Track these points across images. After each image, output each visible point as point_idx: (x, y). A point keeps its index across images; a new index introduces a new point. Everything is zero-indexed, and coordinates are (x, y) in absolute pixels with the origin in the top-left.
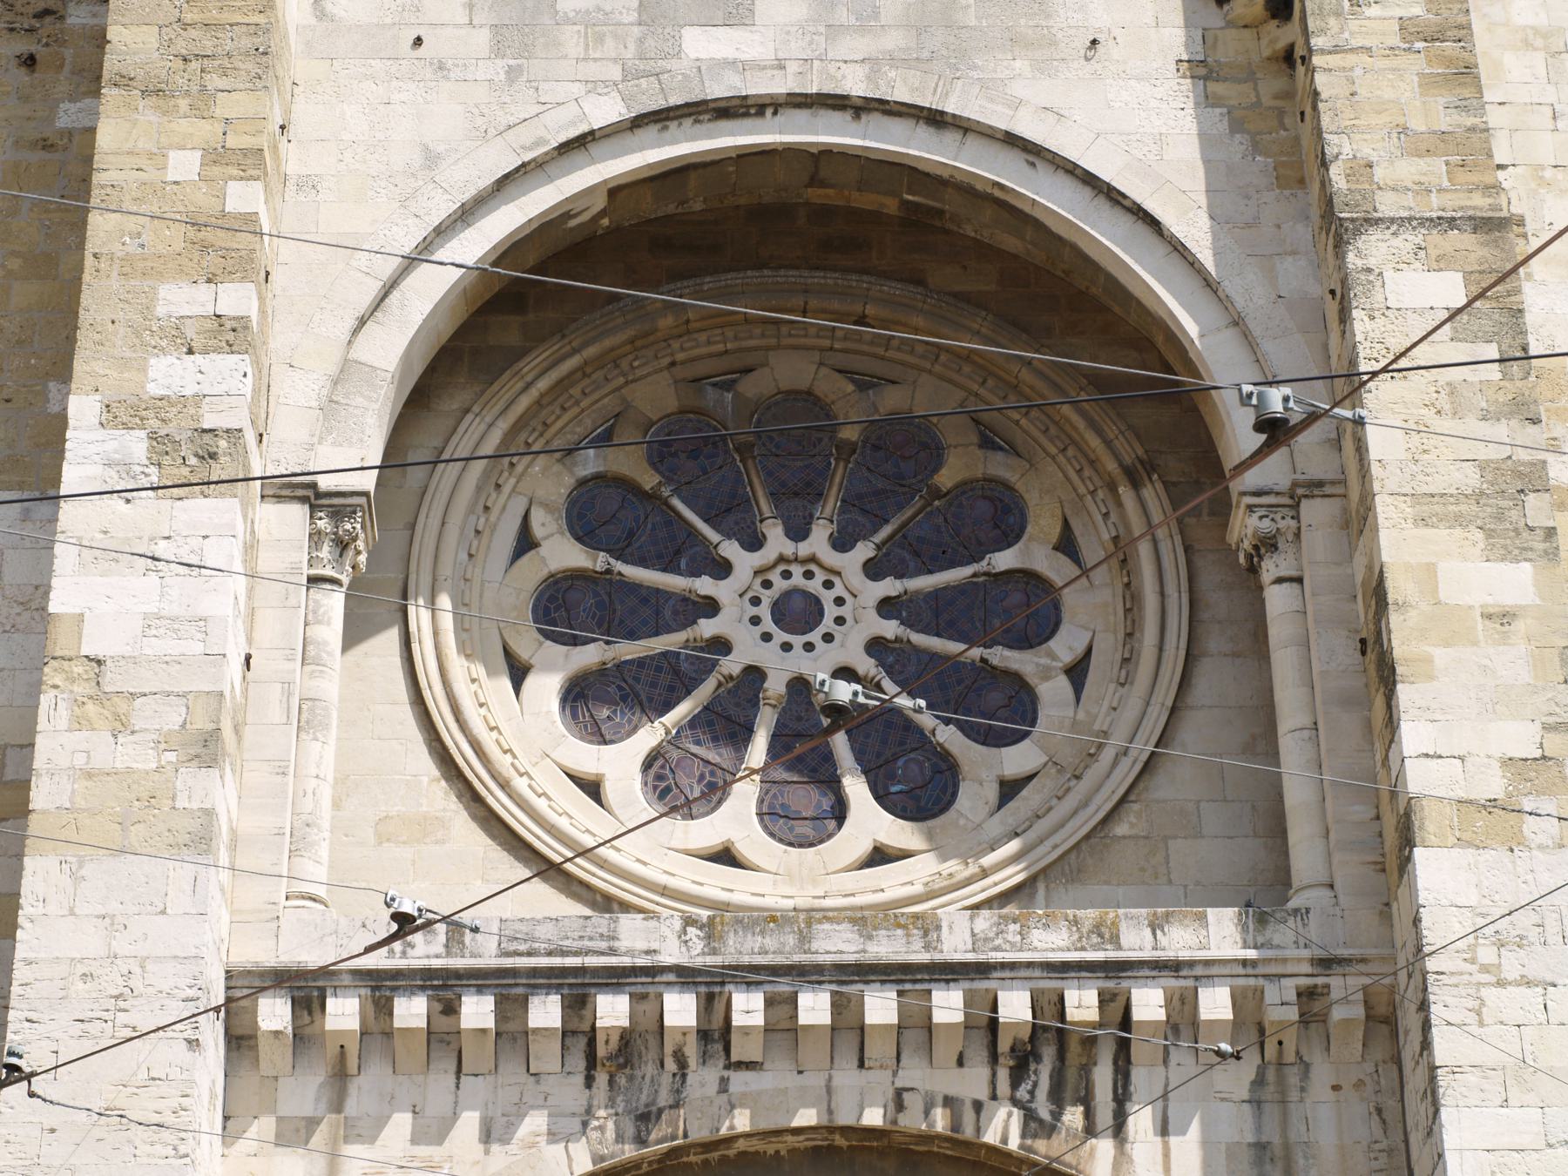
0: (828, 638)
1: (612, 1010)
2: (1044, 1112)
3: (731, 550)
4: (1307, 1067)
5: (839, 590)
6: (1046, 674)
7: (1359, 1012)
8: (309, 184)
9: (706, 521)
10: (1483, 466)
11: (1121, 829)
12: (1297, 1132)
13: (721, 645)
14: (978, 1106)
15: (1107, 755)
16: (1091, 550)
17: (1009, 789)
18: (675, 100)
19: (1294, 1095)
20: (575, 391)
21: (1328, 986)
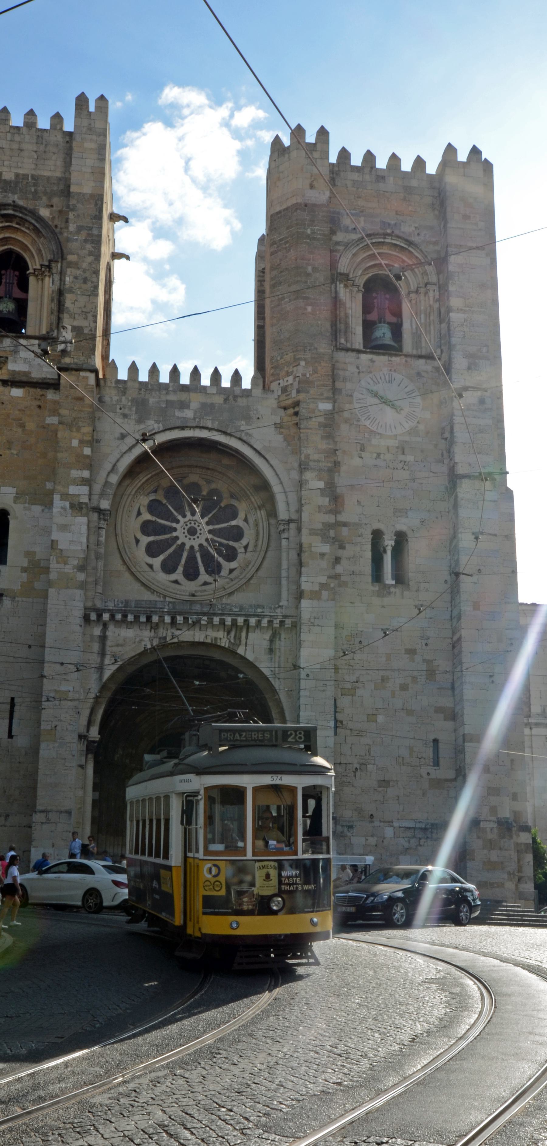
0: (198, 537)
1: (155, 619)
2: (232, 641)
3: (180, 517)
4: (280, 634)
5: (201, 527)
6: (240, 548)
7: (290, 626)
8: (98, 441)
9: (175, 510)
10: (323, 523)
11: (252, 582)
12: (277, 647)
13: (177, 538)
14: (220, 639)
15: (250, 567)
16: (251, 520)
17: (231, 571)
18: (173, 426)
19: (277, 639)
20: (150, 481)
21: (284, 621)
